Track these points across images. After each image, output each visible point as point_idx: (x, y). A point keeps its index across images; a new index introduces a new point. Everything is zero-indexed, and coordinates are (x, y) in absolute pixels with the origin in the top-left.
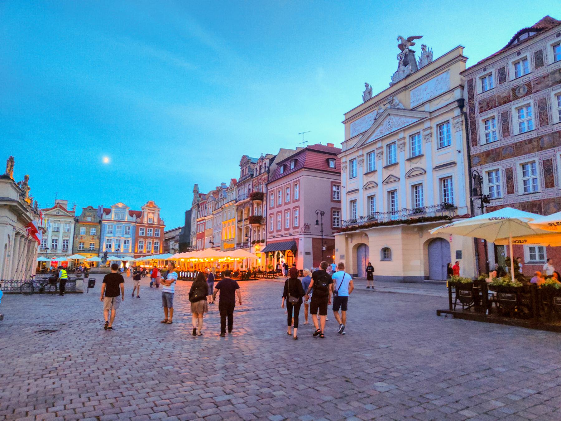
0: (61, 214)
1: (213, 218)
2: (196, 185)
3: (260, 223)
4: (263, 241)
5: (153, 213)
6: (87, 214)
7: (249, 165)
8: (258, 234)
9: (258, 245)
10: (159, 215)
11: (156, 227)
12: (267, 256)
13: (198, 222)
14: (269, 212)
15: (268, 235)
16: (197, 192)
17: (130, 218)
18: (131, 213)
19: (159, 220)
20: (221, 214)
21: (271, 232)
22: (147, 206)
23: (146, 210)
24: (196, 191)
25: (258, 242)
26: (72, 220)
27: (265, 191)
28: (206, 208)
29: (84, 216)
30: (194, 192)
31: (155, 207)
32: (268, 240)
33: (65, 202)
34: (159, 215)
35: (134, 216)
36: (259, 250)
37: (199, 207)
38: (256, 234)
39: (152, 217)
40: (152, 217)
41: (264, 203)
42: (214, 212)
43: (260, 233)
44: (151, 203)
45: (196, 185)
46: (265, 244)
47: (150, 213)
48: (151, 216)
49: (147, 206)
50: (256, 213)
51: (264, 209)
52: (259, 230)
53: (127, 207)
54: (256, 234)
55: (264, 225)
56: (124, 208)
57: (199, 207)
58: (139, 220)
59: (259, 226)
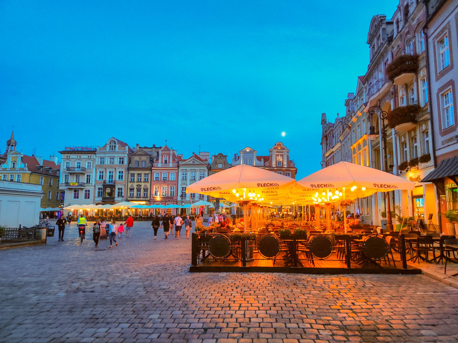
0: (196, 163)
1: (341, 146)
2: (324, 115)
3: (414, 121)
4: (425, 158)
5: (282, 155)
6: (218, 161)
7: (384, 26)
8: (411, 147)
9: (413, 169)
10: (288, 157)
11: (286, 170)
12: (441, 191)
13: (327, 157)
14: (436, 86)
15: (440, 139)
16: (325, 122)
17: (259, 162)
18: (259, 158)
19: (289, 162)
20: (349, 136)
21: (444, 133)
22: (275, 148)
23: (274, 153)
24: (324, 121)
25: (414, 163)
26: (206, 168)
27: (420, 49)
28: (333, 137)
29: (216, 163)
30: (322, 124)
31: (284, 149)
32: (438, 153)
33: (207, 154)
34: (288, 157)
35: (262, 160)
36: (417, 179)
37: (327, 140)
38: (407, 149)
39: (281, 160)
40: (281, 160)
41: (423, 73)
42: (341, 138)
43: (418, 144)
44: (279, 145)
45: (324, 115)
46: (431, 162)
47: (278, 155)
48: (280, 159)
49: (275, 148)
50: (403, 104)
51: (423, 87)
52: (414, 139)
53: (255, 151)
54: (407, 149)
55: (425, 121)
56: (252, 152)
57: (327, 140)
58: (267, 164)
59: (414, 130)
